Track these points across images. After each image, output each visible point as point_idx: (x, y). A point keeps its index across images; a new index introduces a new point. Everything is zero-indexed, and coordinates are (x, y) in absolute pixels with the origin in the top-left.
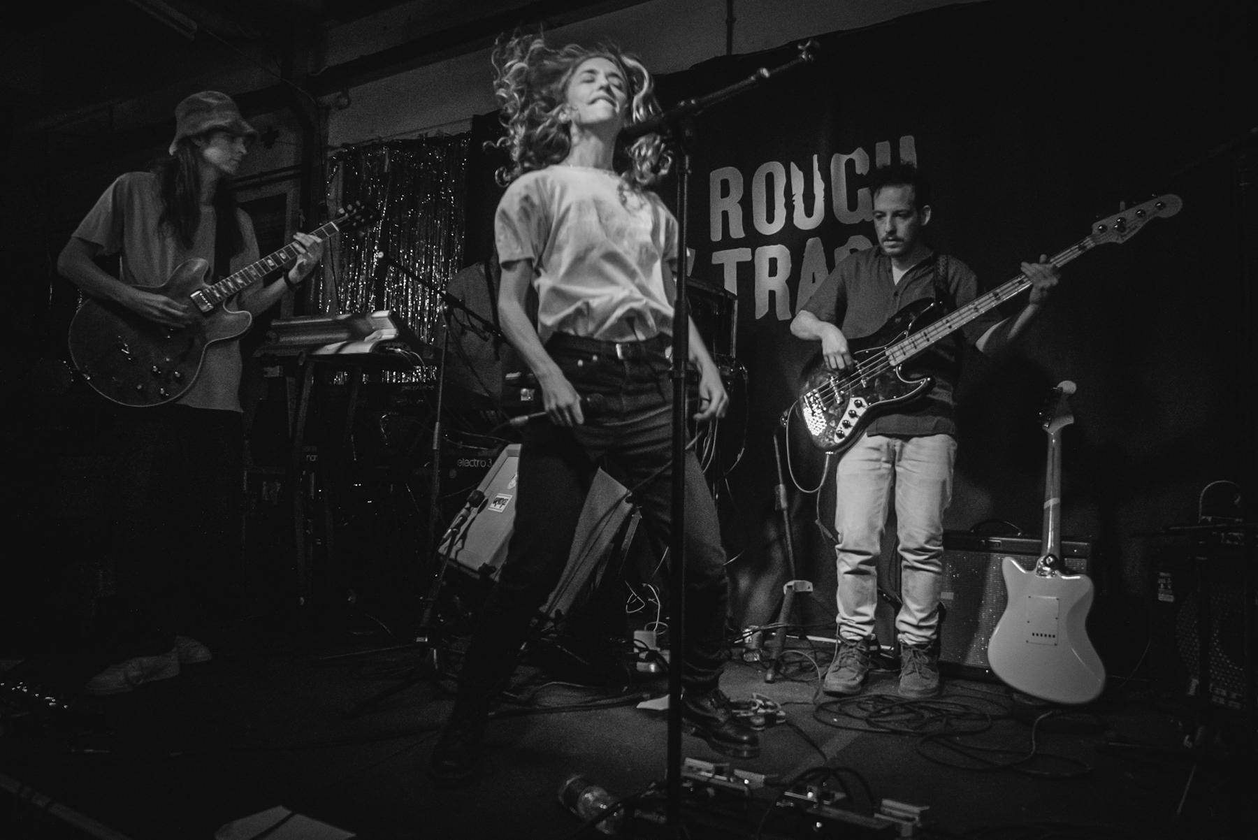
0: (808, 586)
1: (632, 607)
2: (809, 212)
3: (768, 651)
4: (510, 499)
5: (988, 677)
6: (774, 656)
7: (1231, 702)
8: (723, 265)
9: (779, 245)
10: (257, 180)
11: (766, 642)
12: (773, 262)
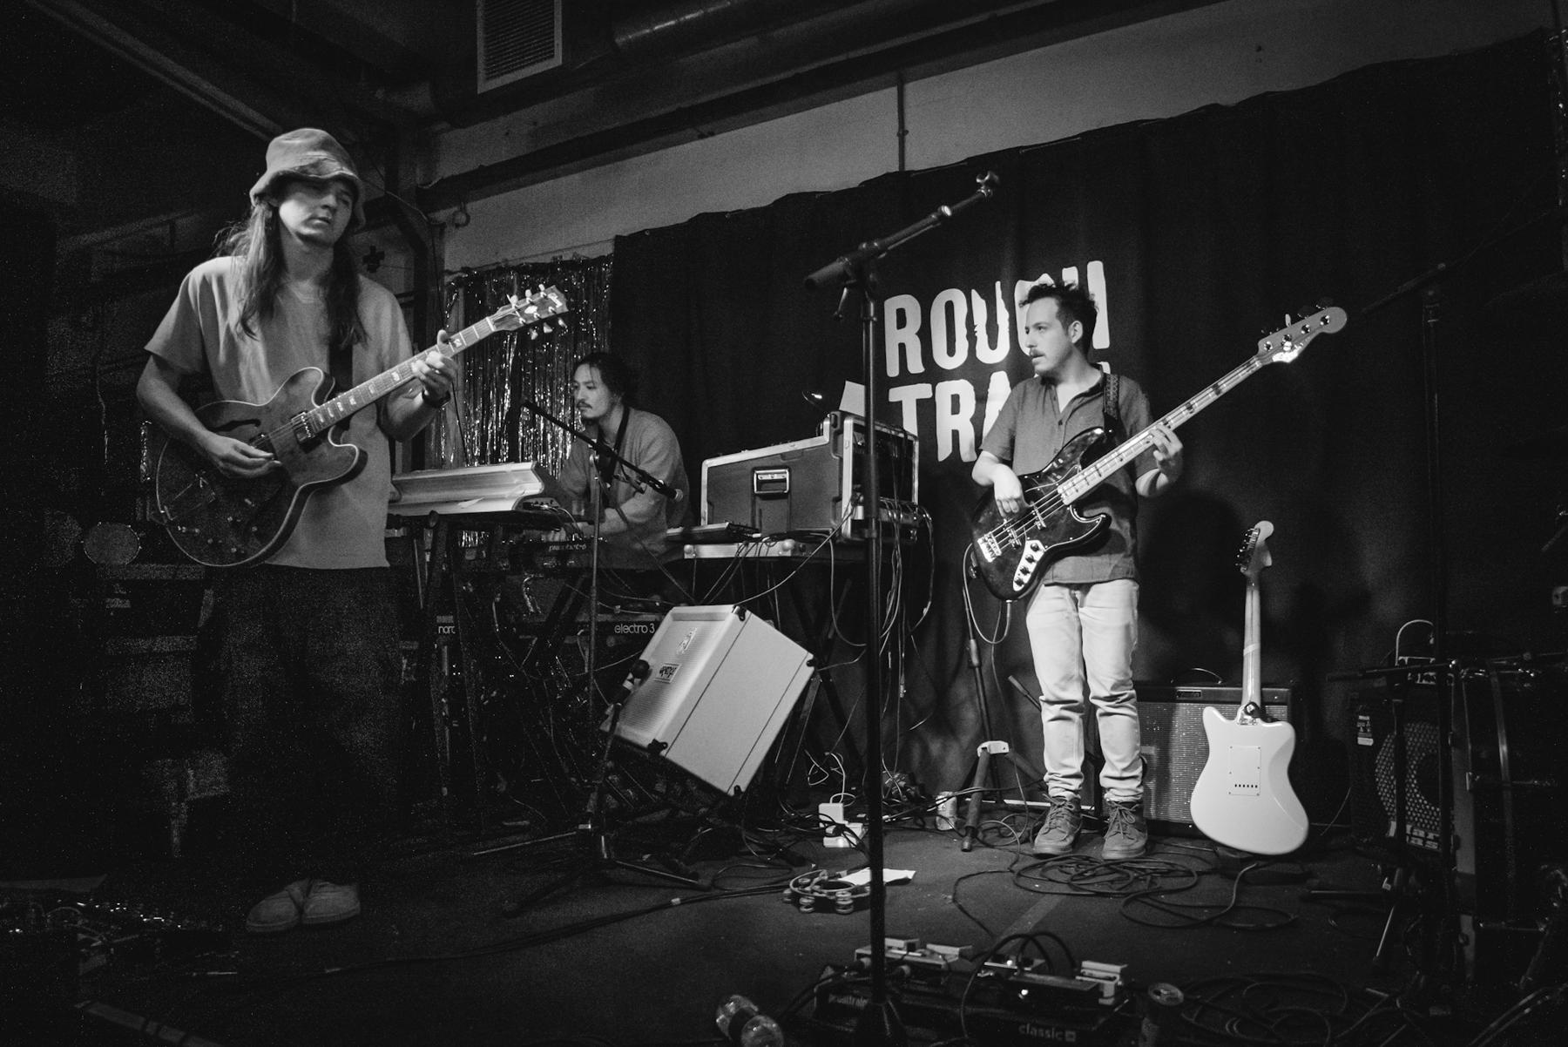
0: (1000, 747)
1: (814, 778)
3: (964, 818)
5: (1191, 833)
6: (970, 823)
7: (1428, 842)
8: (901, 402)
12: (955, 399)
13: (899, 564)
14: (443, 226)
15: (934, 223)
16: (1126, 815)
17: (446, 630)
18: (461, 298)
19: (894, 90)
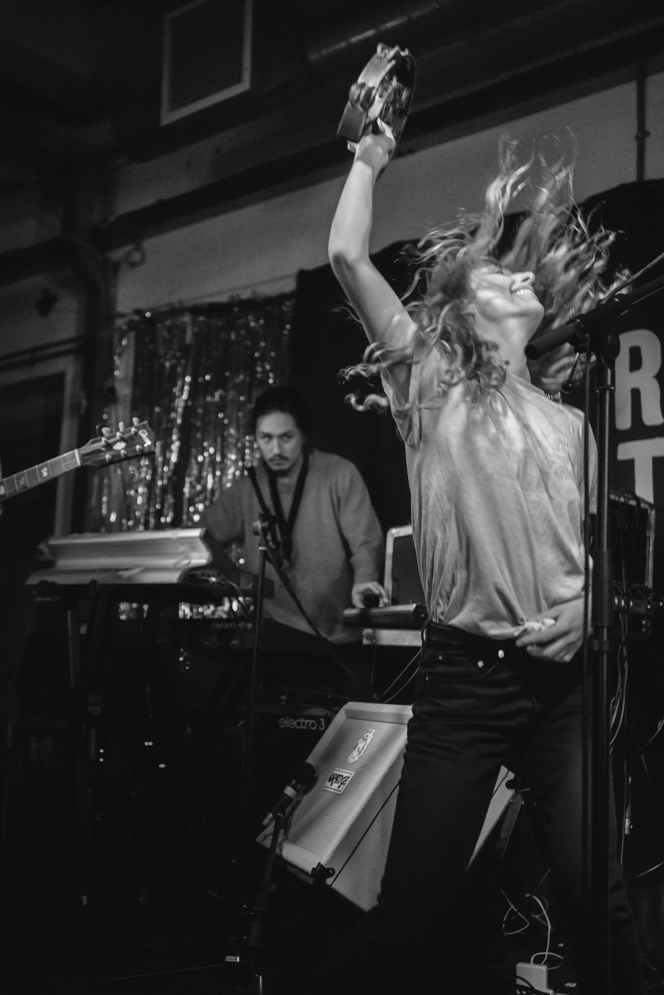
4: (351, 777)
10: (28, 356)
18: (132, 344)
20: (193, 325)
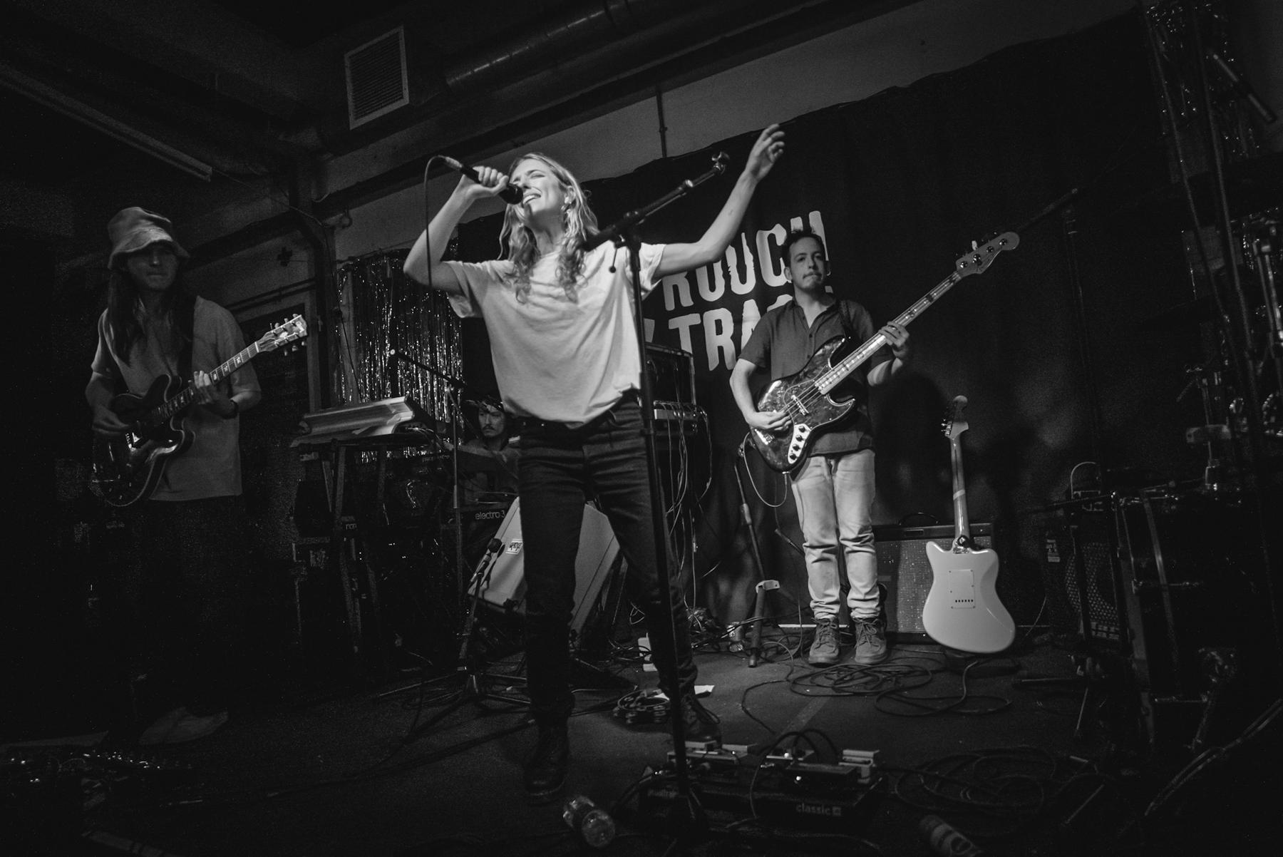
0: (775, 584)
1: (635, 619)
2: (743, 280)
5: (925, 640)
6: (754, 645)
7: (1111, 635)
9: (722, 309)
10: (277, 294)
11: (747, 634)
13: (685, 451)
14: (333, 228)
15: (681, 193)
16: (869, 628)
17: (352, 526)
19: (654, 99)
20: (391, 266)
